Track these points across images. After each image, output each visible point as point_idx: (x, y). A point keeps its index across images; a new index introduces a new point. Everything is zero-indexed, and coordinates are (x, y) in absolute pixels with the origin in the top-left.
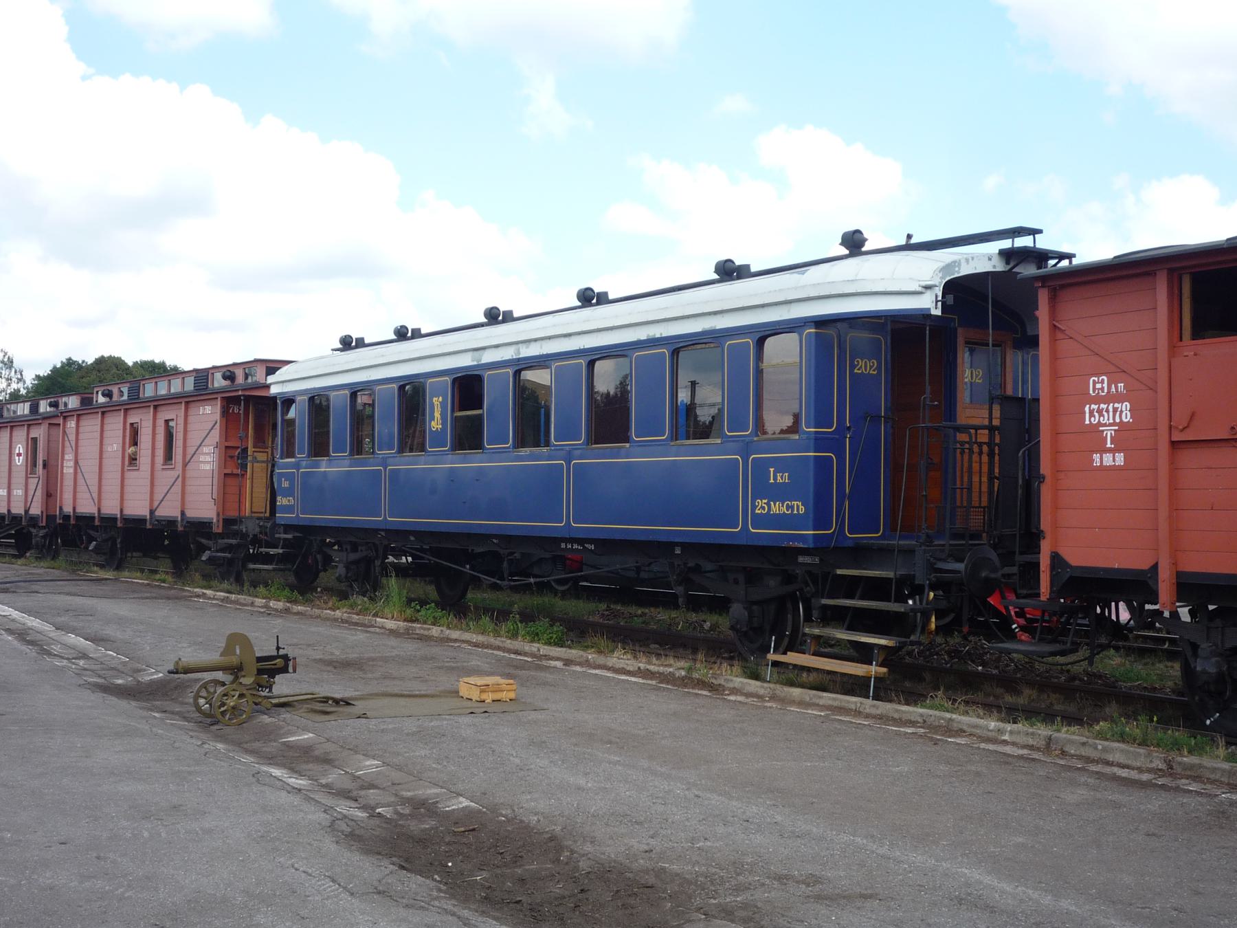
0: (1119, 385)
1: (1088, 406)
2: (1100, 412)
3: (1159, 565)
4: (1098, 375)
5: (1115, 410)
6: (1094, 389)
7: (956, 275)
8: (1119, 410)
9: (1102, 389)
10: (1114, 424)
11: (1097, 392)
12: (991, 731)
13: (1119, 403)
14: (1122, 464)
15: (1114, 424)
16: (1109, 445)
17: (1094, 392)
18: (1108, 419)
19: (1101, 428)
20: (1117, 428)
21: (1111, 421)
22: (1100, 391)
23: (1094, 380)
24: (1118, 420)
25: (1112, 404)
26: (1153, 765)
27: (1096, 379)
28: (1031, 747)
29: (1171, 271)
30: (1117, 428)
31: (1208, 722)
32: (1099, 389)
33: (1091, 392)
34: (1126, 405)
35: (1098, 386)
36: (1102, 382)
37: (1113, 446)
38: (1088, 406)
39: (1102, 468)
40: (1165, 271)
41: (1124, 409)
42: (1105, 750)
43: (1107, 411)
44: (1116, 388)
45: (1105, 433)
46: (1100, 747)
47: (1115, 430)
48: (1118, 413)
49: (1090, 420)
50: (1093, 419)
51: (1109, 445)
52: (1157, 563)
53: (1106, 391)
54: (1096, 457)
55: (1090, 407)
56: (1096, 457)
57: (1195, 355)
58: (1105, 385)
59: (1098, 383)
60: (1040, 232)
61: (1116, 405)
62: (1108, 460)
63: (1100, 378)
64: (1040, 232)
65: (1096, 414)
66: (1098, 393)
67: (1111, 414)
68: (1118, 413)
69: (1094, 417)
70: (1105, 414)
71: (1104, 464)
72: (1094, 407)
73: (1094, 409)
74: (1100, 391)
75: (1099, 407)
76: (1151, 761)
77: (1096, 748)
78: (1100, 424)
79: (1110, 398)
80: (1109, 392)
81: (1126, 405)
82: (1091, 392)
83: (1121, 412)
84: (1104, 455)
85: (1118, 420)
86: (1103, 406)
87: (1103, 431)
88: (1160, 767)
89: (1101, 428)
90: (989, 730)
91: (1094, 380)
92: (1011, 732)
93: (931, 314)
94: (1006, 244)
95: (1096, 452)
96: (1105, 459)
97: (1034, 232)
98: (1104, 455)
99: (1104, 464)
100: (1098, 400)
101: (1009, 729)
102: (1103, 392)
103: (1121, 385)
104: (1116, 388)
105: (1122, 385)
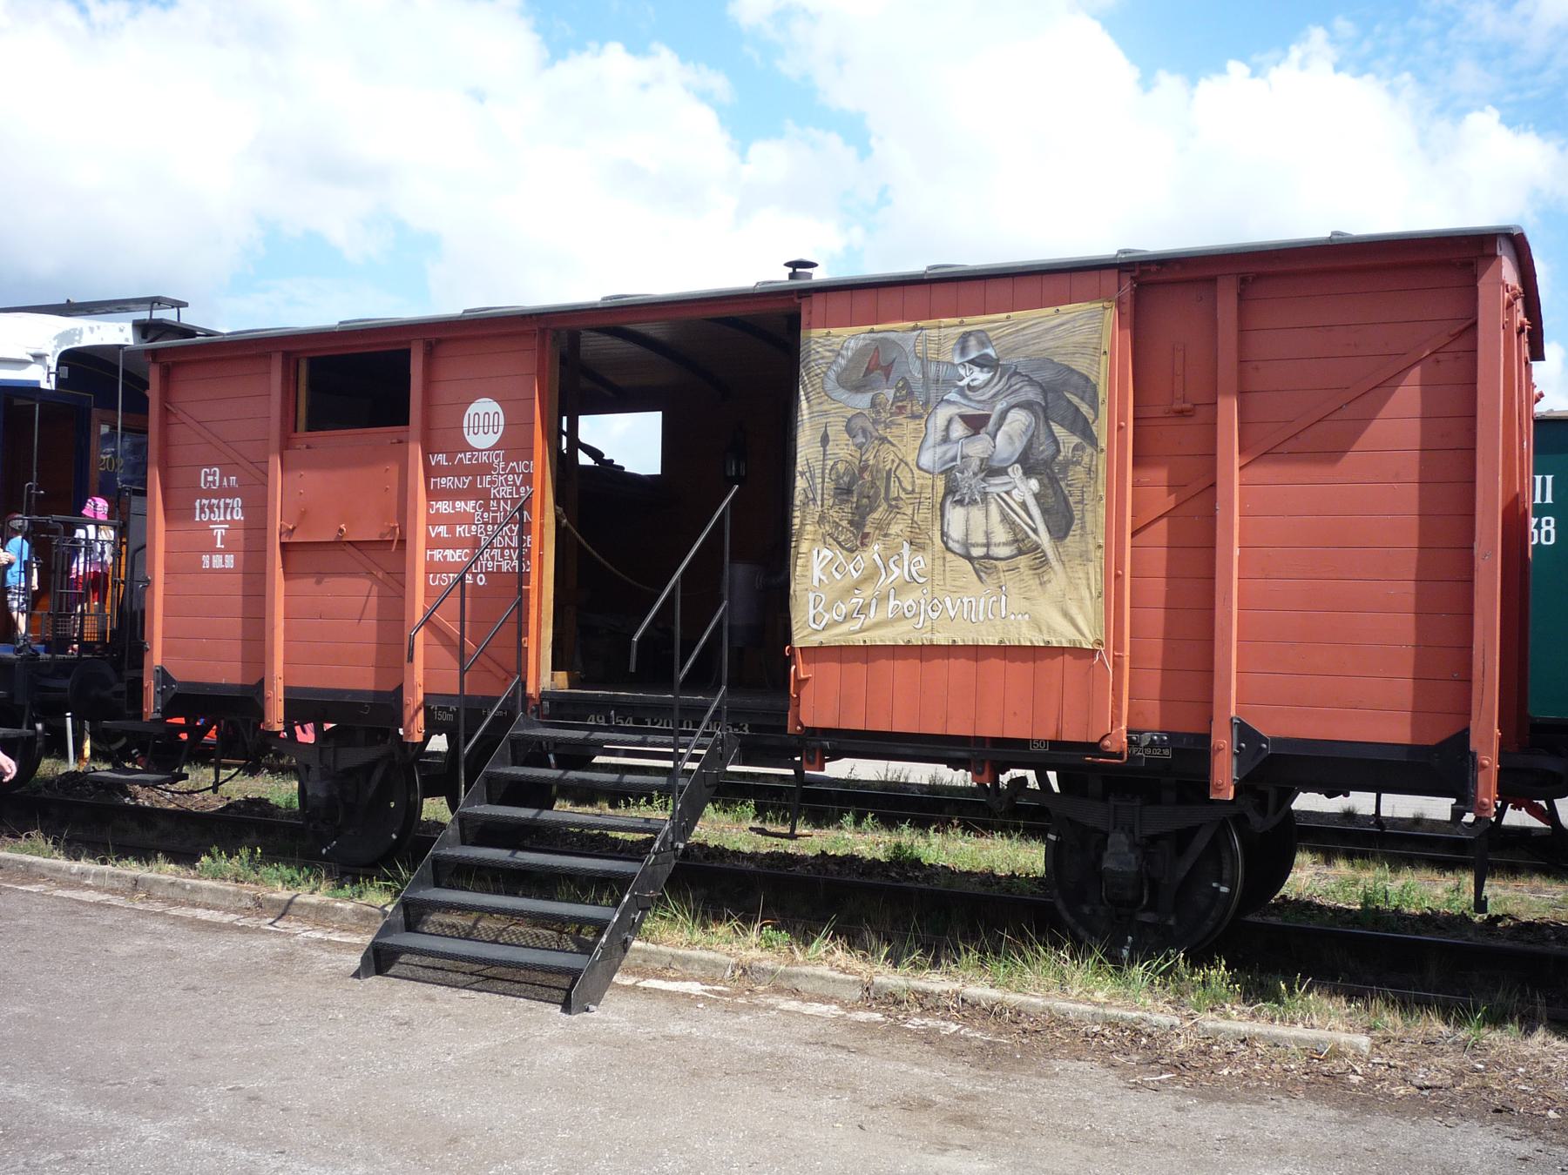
0: (231, 478)
1: (198, 501)
2: (211, 507)
3: (265, 679)
4: (209, 466)
7: (76, 345)
9: (214, 482)
10: (225, 522)
12: (75, 874)
14: (232, 567)
15: (225, 522)
16: (219, 546)
17: (205, 485)
18: (219, 517)
19: (211, 526)
20: (227, 526)
21: (222, 519)
23: (206, 472)
24: (229, 518)
25: (223, 500)
26: (242, 904)
27: (208, 470)
29: (287, 356)
30: (227, 526)
31: (324, 851)
32: (210, 482)
33: (202, 485)
36: (214, 475)
37: (223, 546)
38: (198, 501)
39: (212, 571)
40: (281, 353)
41: (235, 506)
43: (219, 507)
45: (215, 531)
46: (188, 887)
47: (225, 529)
48: (229, 510)
49: (200, 517)
50: (203, 515)
51: (219, 546)
52: (263, 679)
53: (217, 485)
54: (206, 558)
55: (201, 502)
56: (206, 558)
57: (308, 447)
58: (217, 478)
59: (210, 475)
60: (186, 305)
61: (228, 501)
62: (217, 562)
64: (186, 305)
65: (207, 510)
67: (222, 511)
68: (229, 510)
69: (205, 513)
70: (216, 510)
71: (214, 567)
72: (205, 502)
73: (204, 505)
76: (240, 900)
77: (184, 889)
78: (210, 522)
79: (223, 493)
80: (220, 486)
82: (202, 485)
83: (233, 508)
84: (214, 557)
85: (229, 518)
86: (214, 501)
87: (213, 529)
88: (248, 906)
89: (211, 526)
90: (71, 874)
91: (206, 472)
93: (40, 388)
94: (144, 315)
95: (206, 552)
96: (214, 561)
97: (179, 305)
98: (214, 557)
99: (214, 567)
100: (209, 494)
102: (215, 486)
103: (233, 478)
105: (234, 478)
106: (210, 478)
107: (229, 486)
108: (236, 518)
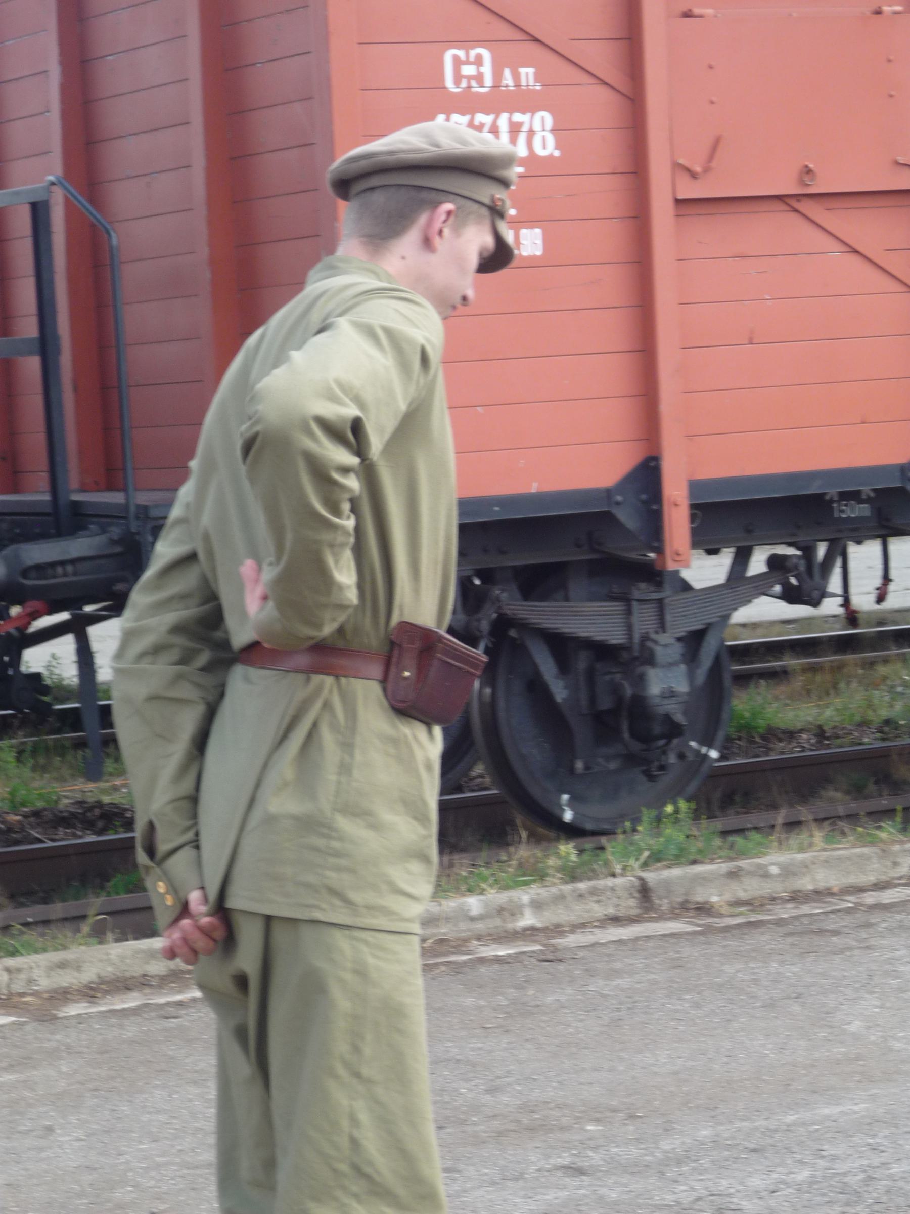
0: (523, 71)
4: (466, 43)
5: (515, 129)
6: (458, 78)
8: (525, 128)
9: (479, 78)
11: (464, 84)
13: (524, 113)
14: (539, 252)
17: (457, 82)
22: (474, 83)
27: (461, 53)
28: (616, 920)
32: (469, 78)
33: (449, 83)
34: (543, 119)
35: (468, 70)
36: (479, 61)
42: (788, 872)
44: (516, 77)
46: (774, 870)
53: (488, 81)
58: (487, 70)
59: (468, 63)
61: (518, 117)
63: (473, 53)
66: (469, 87)
68: (522, 138)
74: (474, 83)
75: (472, 120)
76: (895, 864)
77: (766, 875)
80: (497, 85)
81: (543, 119)
83: (531, 133)
86: (480, 118)
90: (473, 919)
92: (537, 906)
101: (526, 899)
102: (481, 84)
103: (527, 74)
104: (516, 77)
105: (531, 71)
106: (468, 70)
107: (518, 85)
108: (540, 151)
